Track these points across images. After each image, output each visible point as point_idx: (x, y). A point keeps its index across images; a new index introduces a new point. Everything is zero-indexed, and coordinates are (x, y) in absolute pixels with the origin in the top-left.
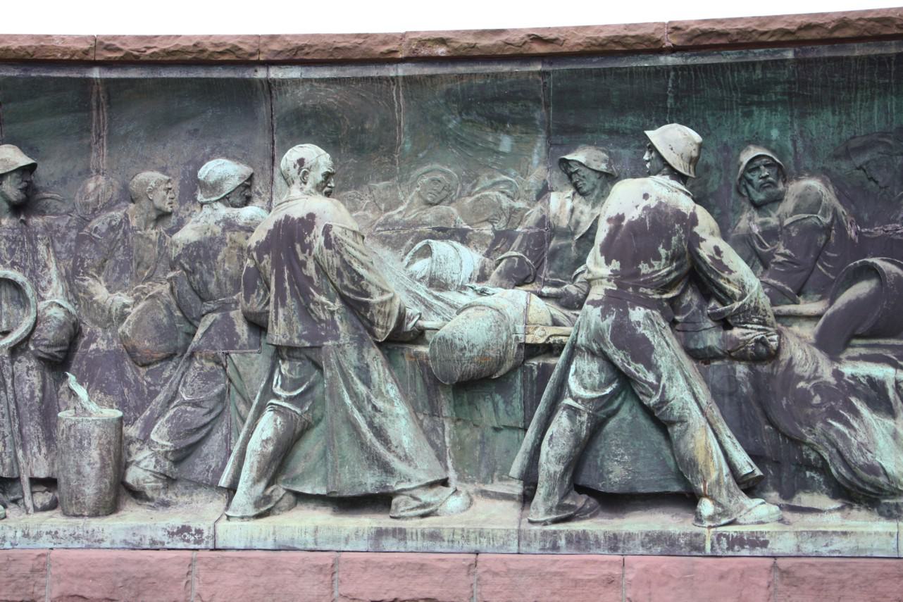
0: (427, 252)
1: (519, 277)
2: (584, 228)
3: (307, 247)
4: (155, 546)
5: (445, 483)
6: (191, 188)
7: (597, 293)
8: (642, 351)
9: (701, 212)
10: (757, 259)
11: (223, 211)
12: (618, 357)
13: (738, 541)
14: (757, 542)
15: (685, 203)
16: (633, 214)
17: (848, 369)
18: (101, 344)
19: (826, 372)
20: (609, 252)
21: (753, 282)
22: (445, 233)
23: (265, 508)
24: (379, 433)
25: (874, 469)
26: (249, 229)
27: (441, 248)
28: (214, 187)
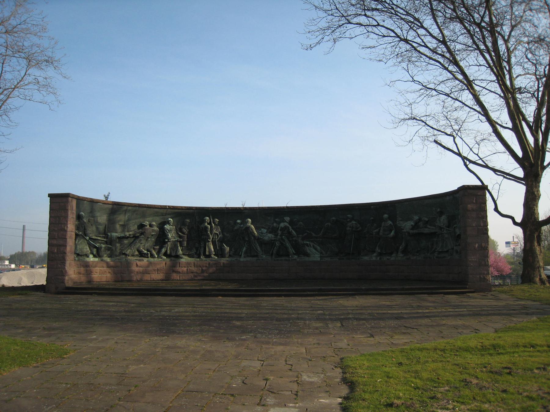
0: (261, 230)
1: (270, 233)
2: (278, 227)
3: (249, 230)
4: (234, 261)
5: (263, 254)
6: (236, 223)
7: (279, 235)
8: (284, 241)
9: (290, 226)
10: (296, 231)
11: (239, 226)
12: (281, 241)
13: (293, 260)
14: (295, 260)
15: (288, 225)
16: (283, 227)
17: (304, 242)
18: (226, 240)
19: (302, 242)
20: (280, 230)
21: (295, 233)
22: (263, 228)
23: (245, 257)
24: (257, 249)
25: (307, 252)
26: (242, 227)
27: (262, 229)
28: (238, 223)
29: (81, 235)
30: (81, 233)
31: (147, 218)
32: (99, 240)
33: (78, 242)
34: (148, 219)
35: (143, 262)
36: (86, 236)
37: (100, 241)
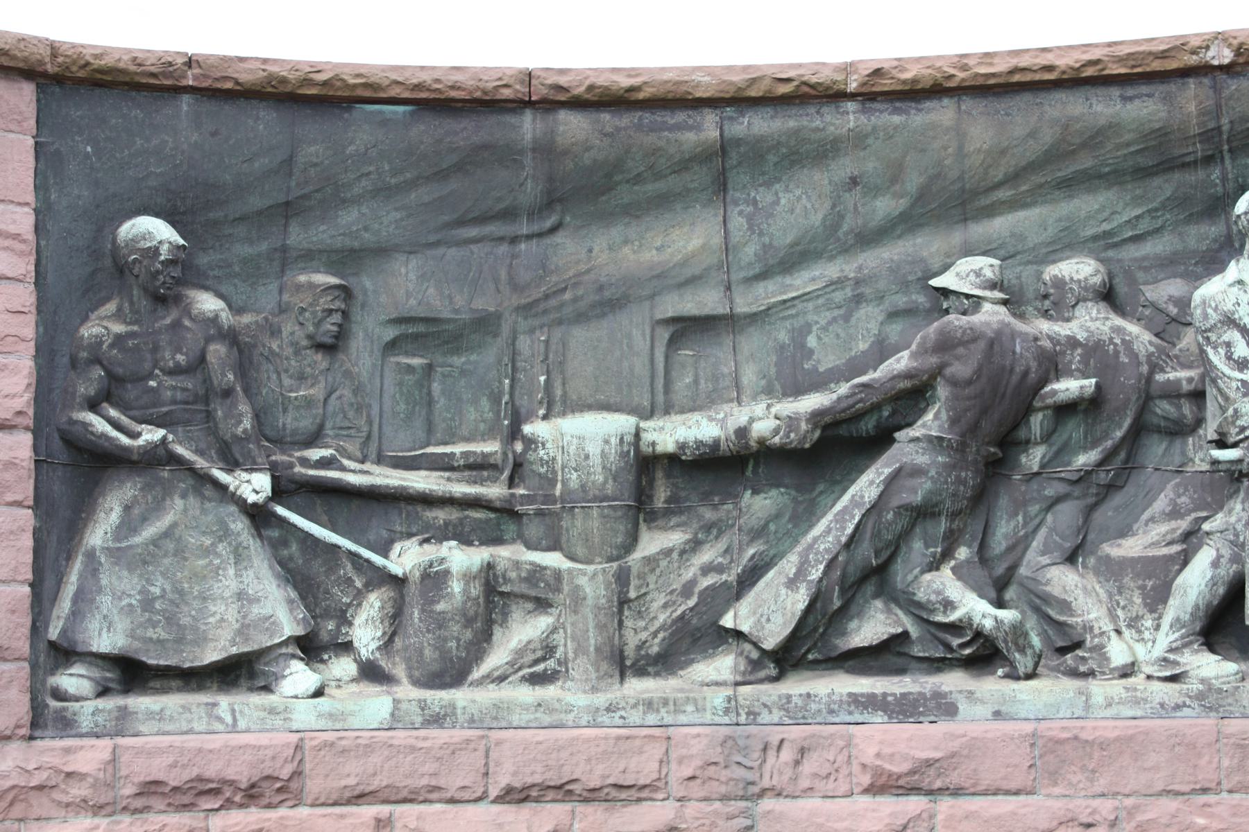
29: (158, 458)
30: (151, 435)
31: (990, 211)
32: (428, 500)
33: (127, 526)
34: (1000, 225)
35: (944, 727)
36: (232, 465)
37: (441, 515)
